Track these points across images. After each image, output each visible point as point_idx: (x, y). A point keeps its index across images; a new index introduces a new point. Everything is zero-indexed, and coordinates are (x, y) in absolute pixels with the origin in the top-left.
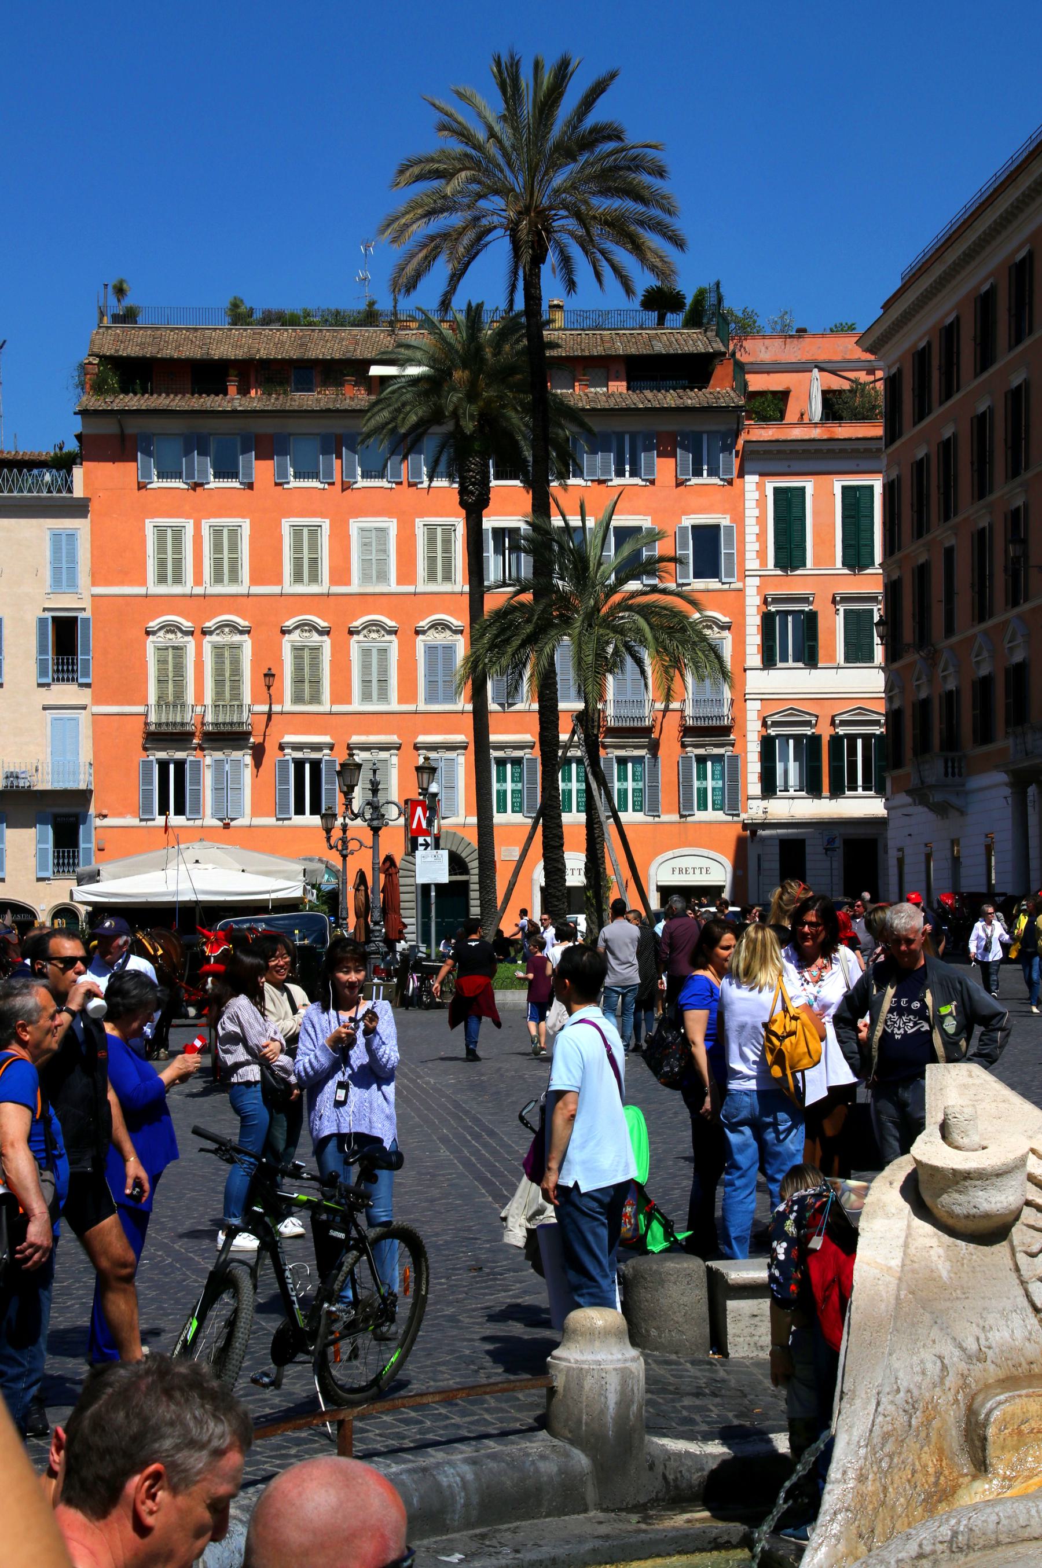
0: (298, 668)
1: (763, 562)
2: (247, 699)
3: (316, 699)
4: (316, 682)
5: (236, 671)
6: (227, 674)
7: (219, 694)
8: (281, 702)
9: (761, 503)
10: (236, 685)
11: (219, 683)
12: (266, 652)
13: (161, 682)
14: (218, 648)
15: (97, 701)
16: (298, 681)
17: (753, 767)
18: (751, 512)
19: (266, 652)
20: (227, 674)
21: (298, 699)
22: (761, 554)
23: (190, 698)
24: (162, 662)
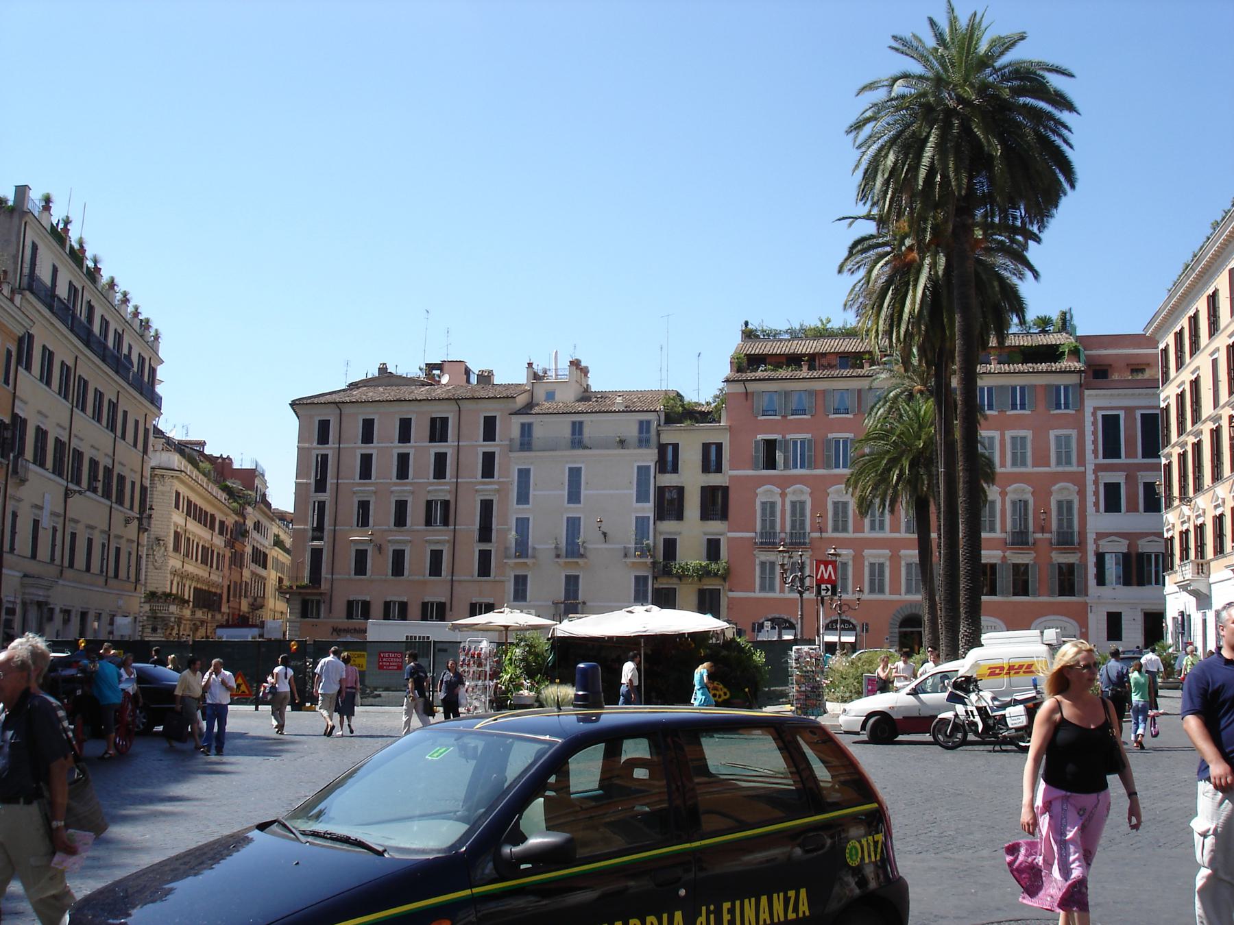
0: (836, 514)
1: (1096, 457)
2: (808, 528)
3: (845, 529)
4: (845, 523)
5: (803, 514)
6: (798, 515)
7: (793, 527)
8: (827, 532)
9: (1094, 423)
10: (803, 523)
11: (793, 522)
12: (819, 504)
13: (763, 521)
14: (793, 504)
15: (729, 531)
16: (835, 522)
17: (1092, 571)
18: (1089, 428)
19: (819, 504)
20: (798, 515)
21: (835, 529)
22: (1095, 452)
23: (778, 529)
24: (764, 510)
